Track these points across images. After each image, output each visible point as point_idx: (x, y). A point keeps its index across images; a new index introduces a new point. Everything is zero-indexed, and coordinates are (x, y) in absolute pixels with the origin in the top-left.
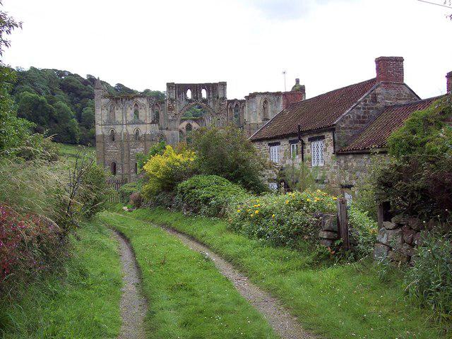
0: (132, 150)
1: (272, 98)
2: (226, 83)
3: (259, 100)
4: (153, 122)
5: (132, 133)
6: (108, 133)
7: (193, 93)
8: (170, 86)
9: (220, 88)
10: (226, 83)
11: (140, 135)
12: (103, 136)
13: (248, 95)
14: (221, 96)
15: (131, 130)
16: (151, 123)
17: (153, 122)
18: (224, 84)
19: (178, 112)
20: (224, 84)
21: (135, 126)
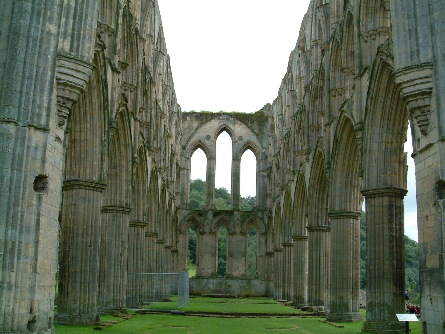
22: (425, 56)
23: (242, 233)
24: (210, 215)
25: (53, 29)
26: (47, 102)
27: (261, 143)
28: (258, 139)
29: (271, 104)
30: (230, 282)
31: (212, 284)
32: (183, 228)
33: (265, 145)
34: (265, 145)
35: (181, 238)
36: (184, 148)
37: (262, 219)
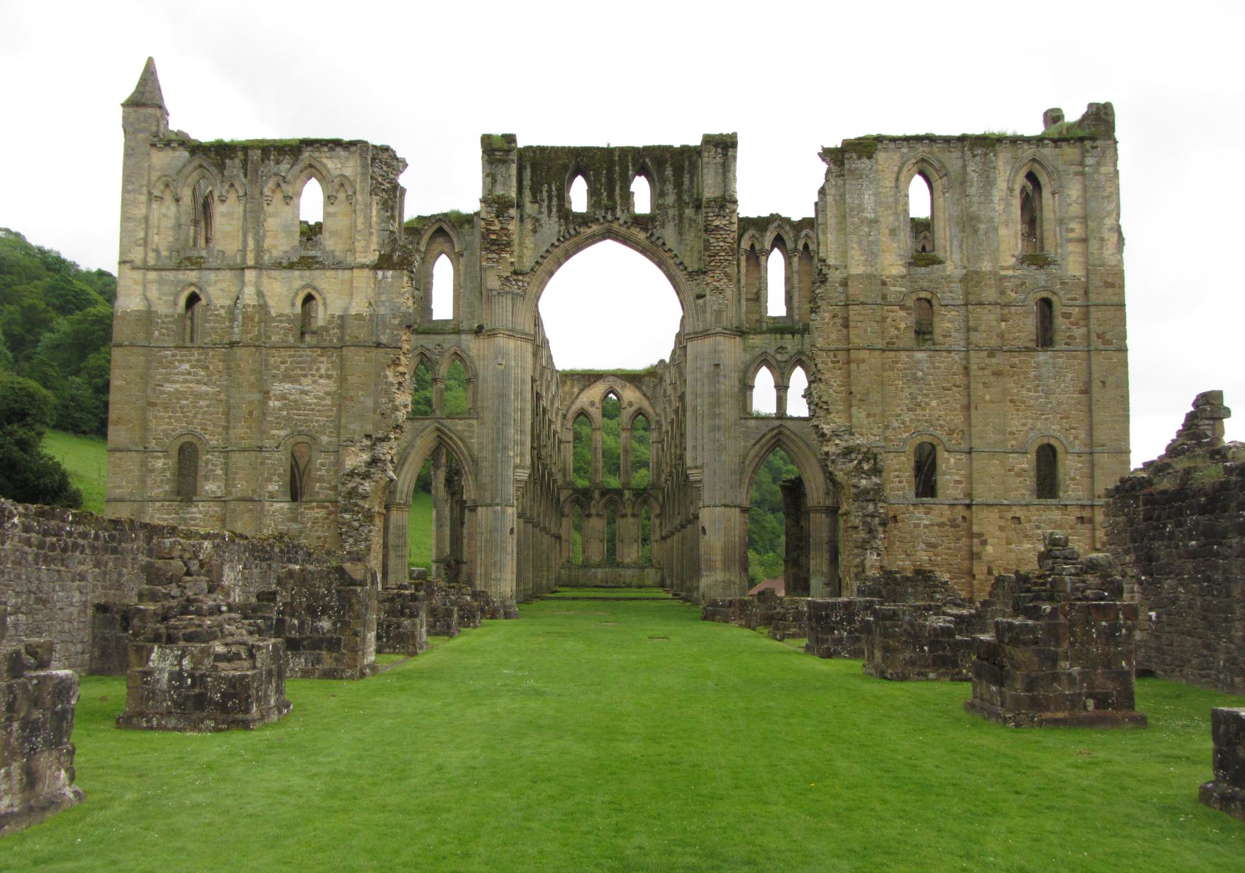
0: (278, 388)
1: (953, 160)
2: (734, 136)
3: (886, 160)
4: (384, 262)
5: (287, 311)
6: (167, 303)
7: (593, 193)
8: (497, 151)
9: (710, 161)
10: (734, 136)
11: (321, 317)
12: (148, 317)
13: (836, 143)
14: (710, 191)
15: (281, 293)
16: (376, 267)
17: (384, 262)
18: (724, 146)
19: (528, 264)
20: (724, 146)
21: (299, 279)
22: (699, 463)
23: (633, 515)
24: (597, 495)
25: (511, 454)
26: (511, 490)
27: (654, 409)
28: (651, 405)
29: (668, 361)
30: (622, 571)
31: (600, 573)
32: (566, 511)
33: (658, 410)
34: (658, 410)
35: (565, 521)
36: (564, 416)
37: (657, 499)
